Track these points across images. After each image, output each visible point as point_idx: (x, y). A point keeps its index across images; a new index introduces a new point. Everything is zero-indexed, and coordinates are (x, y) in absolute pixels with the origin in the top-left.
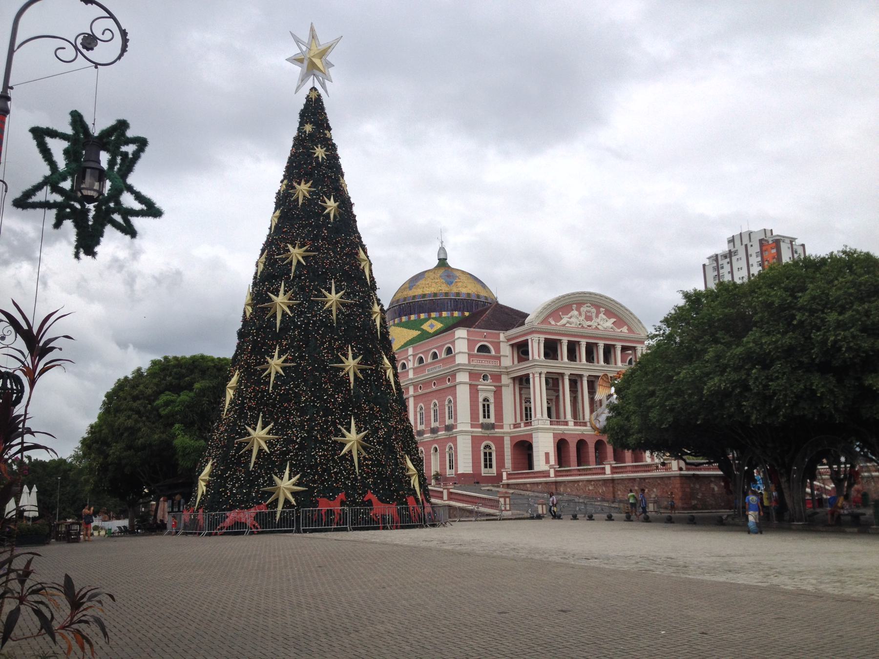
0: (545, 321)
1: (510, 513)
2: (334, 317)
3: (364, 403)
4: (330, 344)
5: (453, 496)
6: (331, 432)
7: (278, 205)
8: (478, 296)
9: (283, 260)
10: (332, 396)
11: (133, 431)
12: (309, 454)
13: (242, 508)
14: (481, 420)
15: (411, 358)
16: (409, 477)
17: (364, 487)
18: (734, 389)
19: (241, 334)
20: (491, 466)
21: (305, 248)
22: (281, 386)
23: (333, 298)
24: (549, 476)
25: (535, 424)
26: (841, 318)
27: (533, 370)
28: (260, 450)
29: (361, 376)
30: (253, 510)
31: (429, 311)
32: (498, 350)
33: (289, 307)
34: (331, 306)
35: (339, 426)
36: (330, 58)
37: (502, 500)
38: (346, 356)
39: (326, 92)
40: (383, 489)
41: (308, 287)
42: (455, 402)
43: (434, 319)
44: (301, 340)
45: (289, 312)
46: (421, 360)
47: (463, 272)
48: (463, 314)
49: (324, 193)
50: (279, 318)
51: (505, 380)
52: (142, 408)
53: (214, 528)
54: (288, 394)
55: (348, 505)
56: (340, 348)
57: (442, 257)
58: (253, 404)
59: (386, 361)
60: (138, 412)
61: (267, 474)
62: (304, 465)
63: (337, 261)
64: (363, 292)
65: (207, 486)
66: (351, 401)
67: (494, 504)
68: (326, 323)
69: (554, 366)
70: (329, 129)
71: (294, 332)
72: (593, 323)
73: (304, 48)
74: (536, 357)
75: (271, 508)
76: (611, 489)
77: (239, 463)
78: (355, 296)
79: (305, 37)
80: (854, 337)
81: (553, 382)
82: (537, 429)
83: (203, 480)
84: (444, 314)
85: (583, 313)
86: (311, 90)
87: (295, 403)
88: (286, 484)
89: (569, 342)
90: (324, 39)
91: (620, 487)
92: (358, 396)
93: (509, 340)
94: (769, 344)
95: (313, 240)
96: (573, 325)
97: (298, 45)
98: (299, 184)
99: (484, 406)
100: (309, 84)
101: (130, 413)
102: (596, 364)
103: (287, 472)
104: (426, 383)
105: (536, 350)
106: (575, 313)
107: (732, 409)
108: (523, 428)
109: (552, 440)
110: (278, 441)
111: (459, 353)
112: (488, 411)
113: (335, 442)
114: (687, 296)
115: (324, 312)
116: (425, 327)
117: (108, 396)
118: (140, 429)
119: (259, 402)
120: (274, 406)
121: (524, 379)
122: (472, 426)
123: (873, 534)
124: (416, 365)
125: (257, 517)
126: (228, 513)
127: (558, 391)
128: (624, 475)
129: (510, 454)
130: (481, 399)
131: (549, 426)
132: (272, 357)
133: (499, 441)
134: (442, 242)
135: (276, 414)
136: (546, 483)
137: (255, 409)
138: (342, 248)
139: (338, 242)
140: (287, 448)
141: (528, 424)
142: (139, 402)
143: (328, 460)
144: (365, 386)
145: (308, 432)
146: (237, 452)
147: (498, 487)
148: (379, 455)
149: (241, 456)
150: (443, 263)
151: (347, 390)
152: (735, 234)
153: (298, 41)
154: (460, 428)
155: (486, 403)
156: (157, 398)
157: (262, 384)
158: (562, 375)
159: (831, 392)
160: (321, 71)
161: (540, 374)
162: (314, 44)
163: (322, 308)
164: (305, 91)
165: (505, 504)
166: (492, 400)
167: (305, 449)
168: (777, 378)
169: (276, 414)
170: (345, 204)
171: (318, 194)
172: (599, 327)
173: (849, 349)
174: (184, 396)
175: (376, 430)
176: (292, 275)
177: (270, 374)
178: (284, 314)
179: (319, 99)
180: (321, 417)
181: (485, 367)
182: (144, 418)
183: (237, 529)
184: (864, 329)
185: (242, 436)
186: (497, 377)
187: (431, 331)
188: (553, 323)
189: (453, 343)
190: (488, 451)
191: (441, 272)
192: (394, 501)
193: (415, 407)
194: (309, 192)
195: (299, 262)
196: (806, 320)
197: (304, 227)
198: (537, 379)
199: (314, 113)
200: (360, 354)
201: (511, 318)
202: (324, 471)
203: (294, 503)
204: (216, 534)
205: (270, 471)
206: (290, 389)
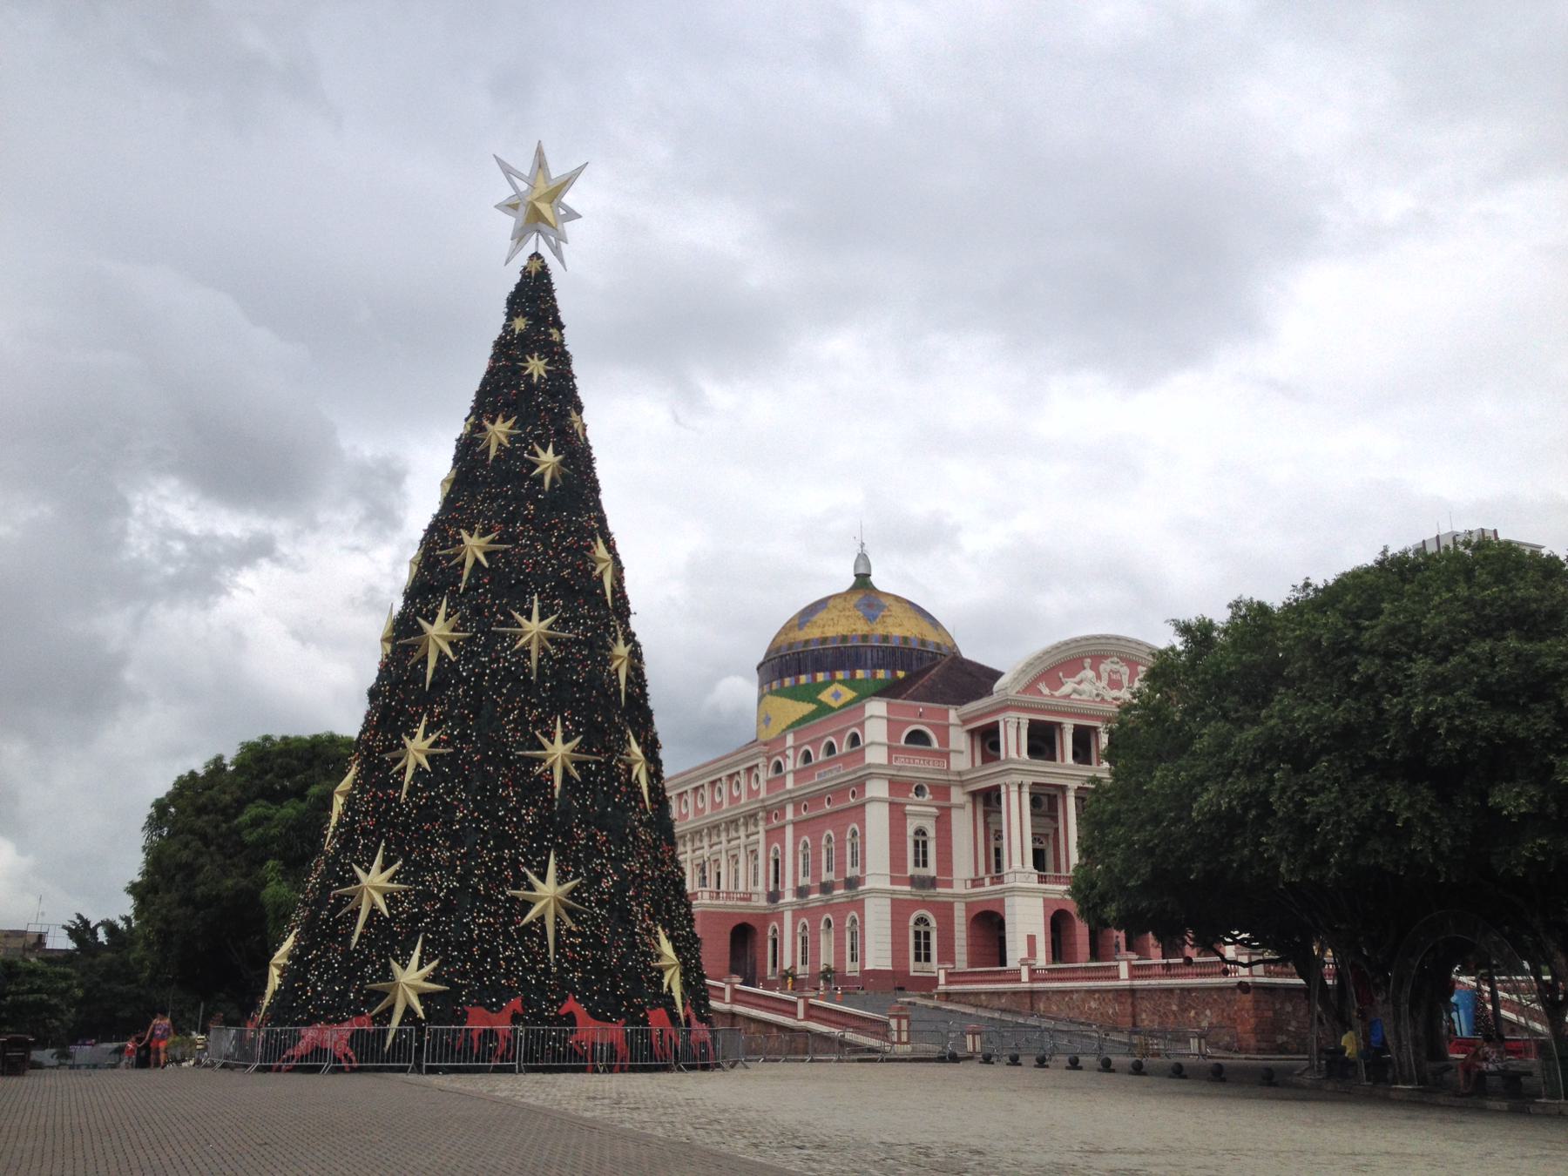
0: (1031, 687)
1: (908, 1048)
2: (534, 664)
3: (578, 826)
4: (521, 714)
5: (814, 1012)
6: (506, 880)
7: (456, 460)
8: (923, 642)
9: (449, 558)
10: (516, 811)
11: (190, 870)
12: (459, 921)
13: (329, 1022)
14: (911, 870)
15: (790, 752)
16: (661, 971)
17: (563, 988)
18: (1246, 808)
19: (373, 694)
20: (928, 959)
21: (490, 537)
22: (422, 790)
23: (534, 627)
24: (1019, 980)
25: (1009, 881)
26: (1440, 669)
27: (1007, 779)
28: (374, 912)
29: (575, 774)
30: (346, 1026)
31: (832, 669)
32: (944, 740)
33: (451, 644)
34: (529, 643)
35: (524, 869)
36: (569, 199)
37: (893, 1023)
38: (550, 736)
39: (562, 261)
40: (599, 992)
41: (490, 607)
42: (863, 836)
43: (842, 682)
44: (467, 706)
45: (450, 653)
46: (807, 757)
47: (897, 599)
48: (894, 673)
49: (538, 438)
50: (432, 663)
51: (957, 796)
52: (209, 830)
53: (274, 1058)
54: (435, 806)
55: (526, 1023)
56: (540, 722)
57: (862, 570)
58: (369, 823)
59: (636, 750)
60: (204, 838)
61: (379, 957)
62: (448, 943)
63: (548, 561)
64: (592, 618)
65: (280, 976)
66: (551, 820)
67: (881, 1029)
68: (516, 677)
70: (560, 326)
71: (456, 688)
73: (523, 186)
74: (1013, 754)
75: (380, 1023)
76: (1129, 1009)
77: (333, 936)
78: (577, 625)
79: (525, 166)
80: (1462, 708)
81: (1045, 802)
82: (1012, 890)
83: (277, 966)
84: (860, 674)
85: (1105, 676)
86: (531, 257)
87: (444, 823)
88: (411, 978)
89: (1077, 728)
90: (556, 171)
91: (1146, 1004)
92: (566, 812)
93: (965, 722)
94: (1308, 720)
95: (506, 522)
97: (509, 179)
98: (493, 422)
99: (916, 843)
100: (530, 248)
101: (190, 837)
102: (1094, 766)
103: (416, 954)
104: (815, 799)
105: (1013, 742)
106: (1089, 673)
107: (1246, 852)
108: (988, 887)
110: (406, 896)
111: (872, 744)
112: (925, 854)
113: (514, 899)
114: (1184, 629)
115: (513, 655)
116: (826, 696)
117: (160, 806)
118: (203, 866)
119: (388, 824)
120: (406, 828)
121: (993, 796)
122: (894, 881)
123: (1537, 1115)
124: (799, 765)
125: (356, 1038)
126: (303, 1030)
127: (1055, 819)
128: (1153, 982)
129: (964, 935)
130: (910, 831)
132: (412, 736)
133: (944, 911)
134: (862, 545)
135: (409, 844)
136: (1015, 993)
137: (372, 832)
138: (561, 538)
139: (554, 527)
140: (421, 909)
141: (998, 879)
142: (206, 818)
143: (495, 934)
144: (583, 793)
145: (460, 879)
146: (332, 914)
147: (931, 997)
148: (598, 927)
149: (338, 922)
150: (863, 581)
151: (546, 800)
152: (1426, 538)
153: (508, 171)
154: (870, 884)
155: (920, 839)
156: (239, 812)
157: (391, 786)
158: (1063, 788)
159: (1426, 819)
160: (549, 224)
161: (1020, 786)
162: (540, 177)
163: (511, 646)
164: (522, 259)
165: (899, 1031)
166: (931, 833)
167: (453, 911)
168: (1323, 788)
169: (409, 844)
170: (578, 458)
171: (524, 440)
173: (1453, 732)
174: (289, 810)
175: (599, 877)
176: (462, 586)
177: (405, 768)
178: (442, 657)
179: (544, 273)
180: (490, 851)
181: (918, 770)
182: (213, 848)
183: (312, 1063)
184: (1484, 692)
185: (344, 883)
186: (942, 791)
187: (835, 704)
188: (1046, 691)
189: (861, 725)
190: (922, 928)
191: (856, 598)
192: (620, 1016)
193: (796, 844)
194: (509, 436)
195: (477, 561)
196: (1377, 673)
197: (493, 498)
199: (533, 296)
200: (578, 733)
201: (973, 680)
202: (485, 954)
203: (421, 1014)
204: (279, 1070)
205: (386, 953)
206: (439, 796)
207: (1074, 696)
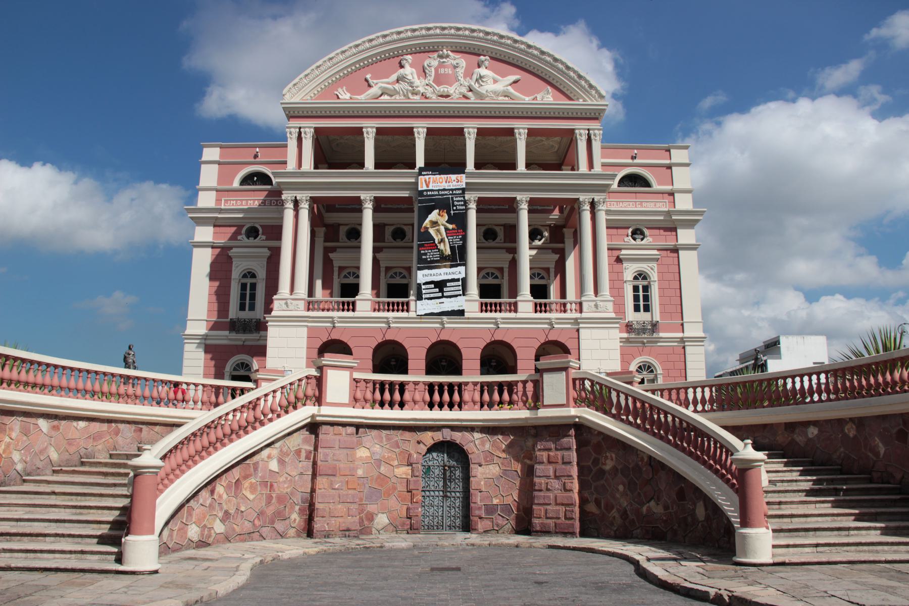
14: (233, 312)
69: (337, 182)
96: (398, 98)
99: (244, 287)
109: (304, 343)
112: (253, 297)
155: (249, 281)
161: (296, 203)
198: (289, 214)
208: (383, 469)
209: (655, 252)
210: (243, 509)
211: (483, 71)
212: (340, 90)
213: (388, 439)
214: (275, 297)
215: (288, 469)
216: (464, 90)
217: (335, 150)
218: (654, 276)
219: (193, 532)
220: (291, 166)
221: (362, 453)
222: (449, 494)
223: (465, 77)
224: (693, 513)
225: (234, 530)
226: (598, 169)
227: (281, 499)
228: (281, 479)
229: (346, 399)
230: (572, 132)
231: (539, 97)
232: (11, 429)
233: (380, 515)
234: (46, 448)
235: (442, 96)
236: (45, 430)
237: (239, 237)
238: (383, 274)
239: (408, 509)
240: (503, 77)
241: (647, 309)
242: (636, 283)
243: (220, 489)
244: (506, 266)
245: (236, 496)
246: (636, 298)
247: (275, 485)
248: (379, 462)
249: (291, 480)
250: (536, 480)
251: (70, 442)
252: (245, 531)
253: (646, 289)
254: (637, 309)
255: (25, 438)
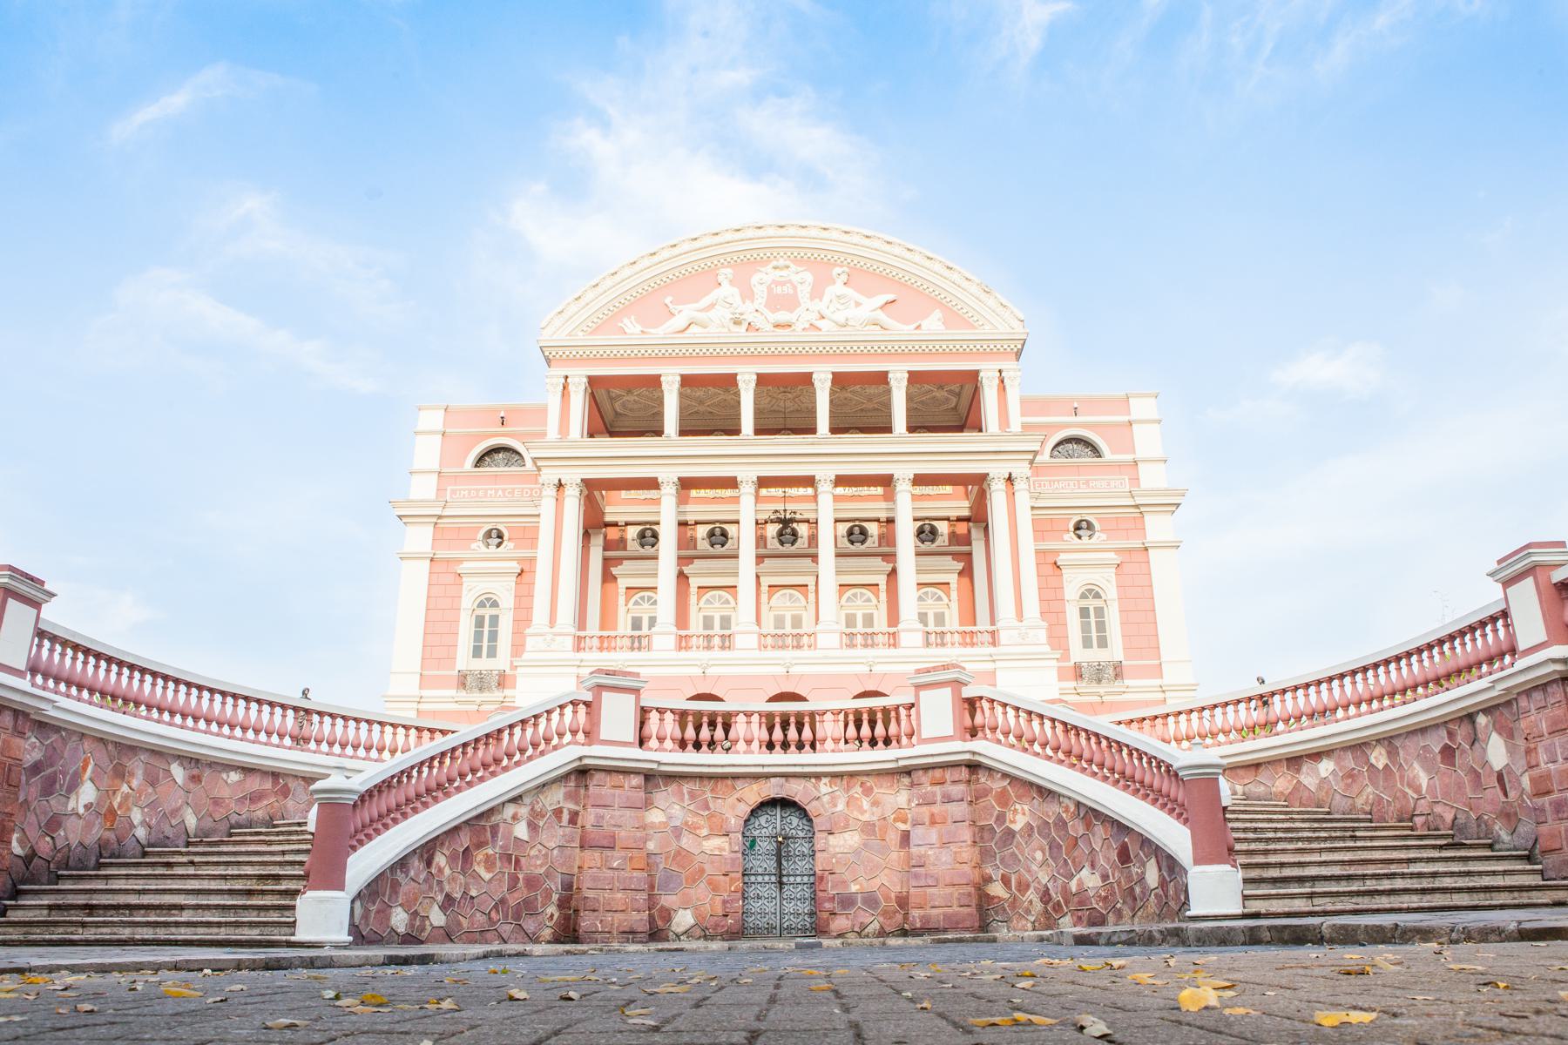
14: (464, 660)
72: (801, 317)
85: (761, 292)
99: (480, 622)
106: (727, 291)
112: (493, 636)
122: (424, 681)
130: (468, 601)
131: (571, 655)
155: (487, 612)
172: (820, 323)
188: (639, 328)
207: (693, 329)
208: (686, 842)
209: (1112, 555)
210: (473, 893)
211: (838, 288)
212: (626, 320)
213: (692, 796)
214: (528, 631)
215: (543, 837)
216: (813, 317)
217: (619, 408)
218: (1111, 592)
219: (399, 919)
220: (553, 432)
221: (655, 816)
222: (785, 879)
223: (812, 298)
224: (1142, 879)
225: (459, 924)
226: (1015, 425)
227: (532, 883)
228: (533, 852)
229: (630, 735)
230: (974, 375)
231: (925, 324)
232: (132, 774)
233: (681, 912)
234: (178, 810)
235: (777, 326)
236: (180, 780)
237: (474, 546)
238: (693, 599)
239: (725, 902)
240: (870, 295)
241: (1103, 643)
242: (1084, 603)
243: (440, 860)
244: (882, 580)
245: (464, 872)
246: (1085, 628)
247: (523, 860)
248: (677, 832)
249: (546, 855)
250: (914, 850)
251: (217, 802)
252: (476, 927)
253: (1100, 612)
254: (1087, 643)
255: (150, 790)
